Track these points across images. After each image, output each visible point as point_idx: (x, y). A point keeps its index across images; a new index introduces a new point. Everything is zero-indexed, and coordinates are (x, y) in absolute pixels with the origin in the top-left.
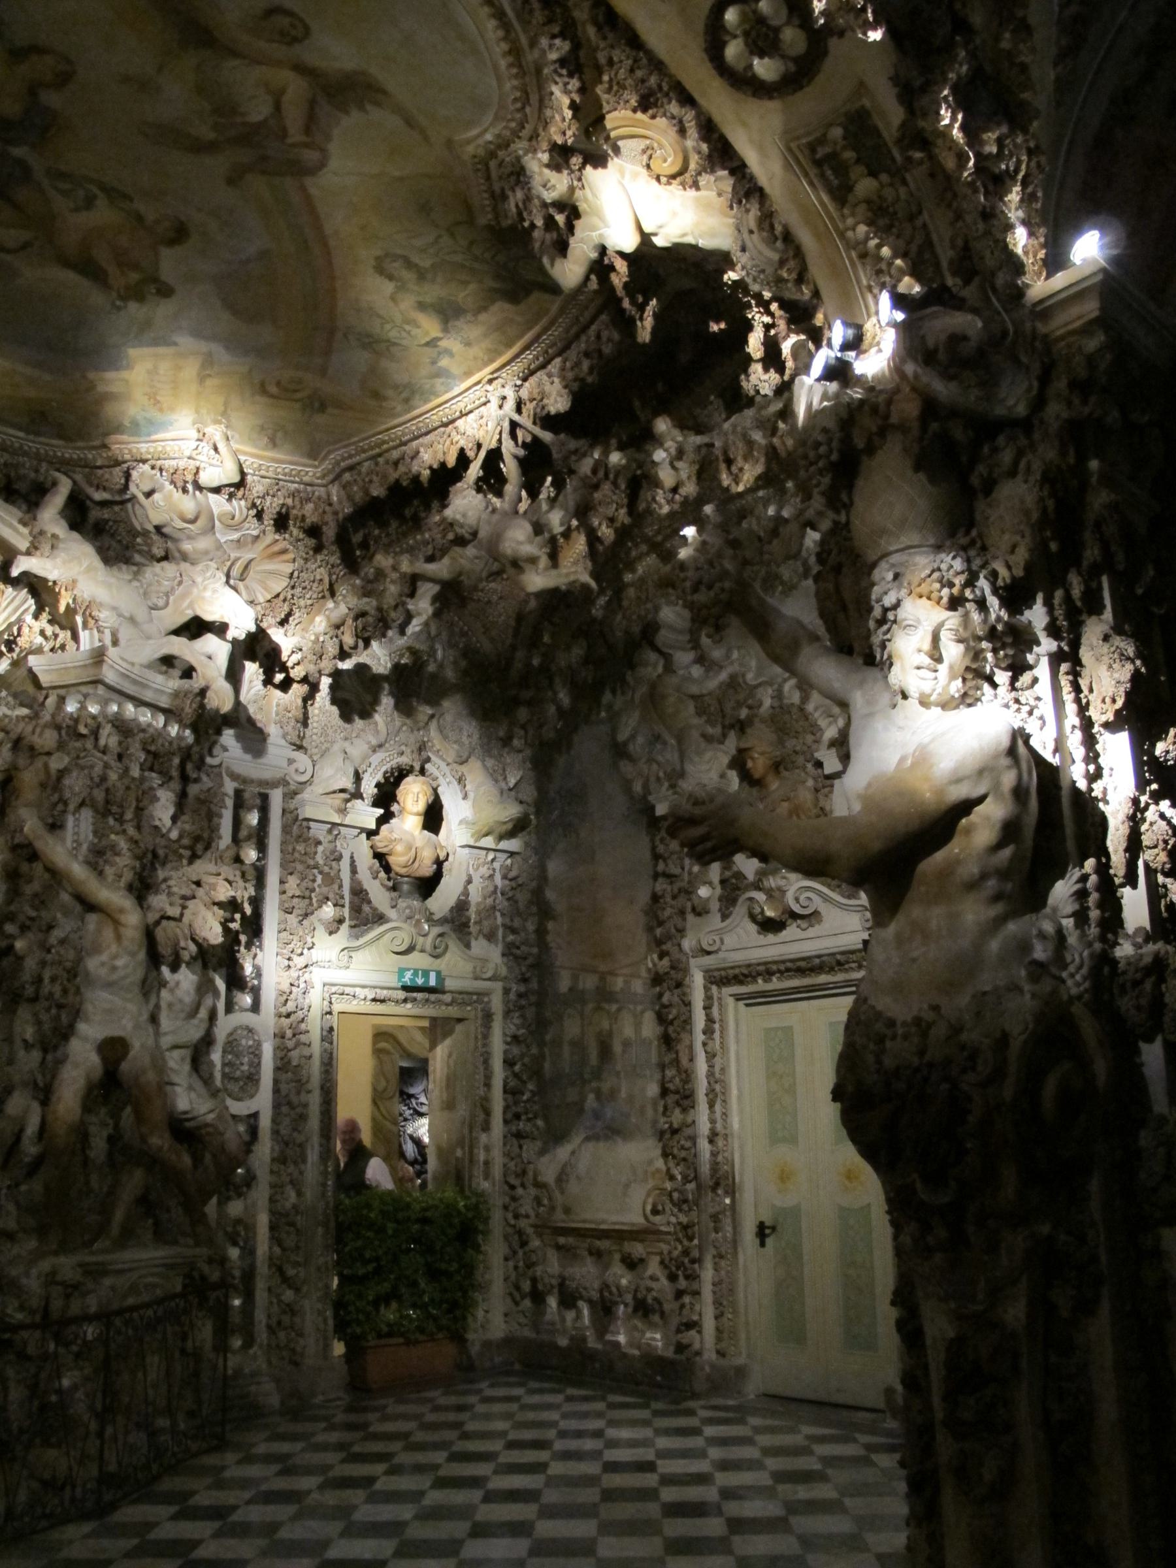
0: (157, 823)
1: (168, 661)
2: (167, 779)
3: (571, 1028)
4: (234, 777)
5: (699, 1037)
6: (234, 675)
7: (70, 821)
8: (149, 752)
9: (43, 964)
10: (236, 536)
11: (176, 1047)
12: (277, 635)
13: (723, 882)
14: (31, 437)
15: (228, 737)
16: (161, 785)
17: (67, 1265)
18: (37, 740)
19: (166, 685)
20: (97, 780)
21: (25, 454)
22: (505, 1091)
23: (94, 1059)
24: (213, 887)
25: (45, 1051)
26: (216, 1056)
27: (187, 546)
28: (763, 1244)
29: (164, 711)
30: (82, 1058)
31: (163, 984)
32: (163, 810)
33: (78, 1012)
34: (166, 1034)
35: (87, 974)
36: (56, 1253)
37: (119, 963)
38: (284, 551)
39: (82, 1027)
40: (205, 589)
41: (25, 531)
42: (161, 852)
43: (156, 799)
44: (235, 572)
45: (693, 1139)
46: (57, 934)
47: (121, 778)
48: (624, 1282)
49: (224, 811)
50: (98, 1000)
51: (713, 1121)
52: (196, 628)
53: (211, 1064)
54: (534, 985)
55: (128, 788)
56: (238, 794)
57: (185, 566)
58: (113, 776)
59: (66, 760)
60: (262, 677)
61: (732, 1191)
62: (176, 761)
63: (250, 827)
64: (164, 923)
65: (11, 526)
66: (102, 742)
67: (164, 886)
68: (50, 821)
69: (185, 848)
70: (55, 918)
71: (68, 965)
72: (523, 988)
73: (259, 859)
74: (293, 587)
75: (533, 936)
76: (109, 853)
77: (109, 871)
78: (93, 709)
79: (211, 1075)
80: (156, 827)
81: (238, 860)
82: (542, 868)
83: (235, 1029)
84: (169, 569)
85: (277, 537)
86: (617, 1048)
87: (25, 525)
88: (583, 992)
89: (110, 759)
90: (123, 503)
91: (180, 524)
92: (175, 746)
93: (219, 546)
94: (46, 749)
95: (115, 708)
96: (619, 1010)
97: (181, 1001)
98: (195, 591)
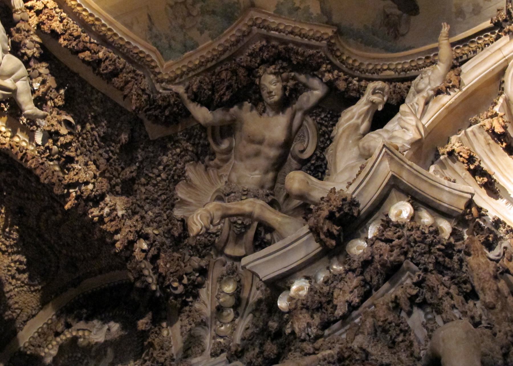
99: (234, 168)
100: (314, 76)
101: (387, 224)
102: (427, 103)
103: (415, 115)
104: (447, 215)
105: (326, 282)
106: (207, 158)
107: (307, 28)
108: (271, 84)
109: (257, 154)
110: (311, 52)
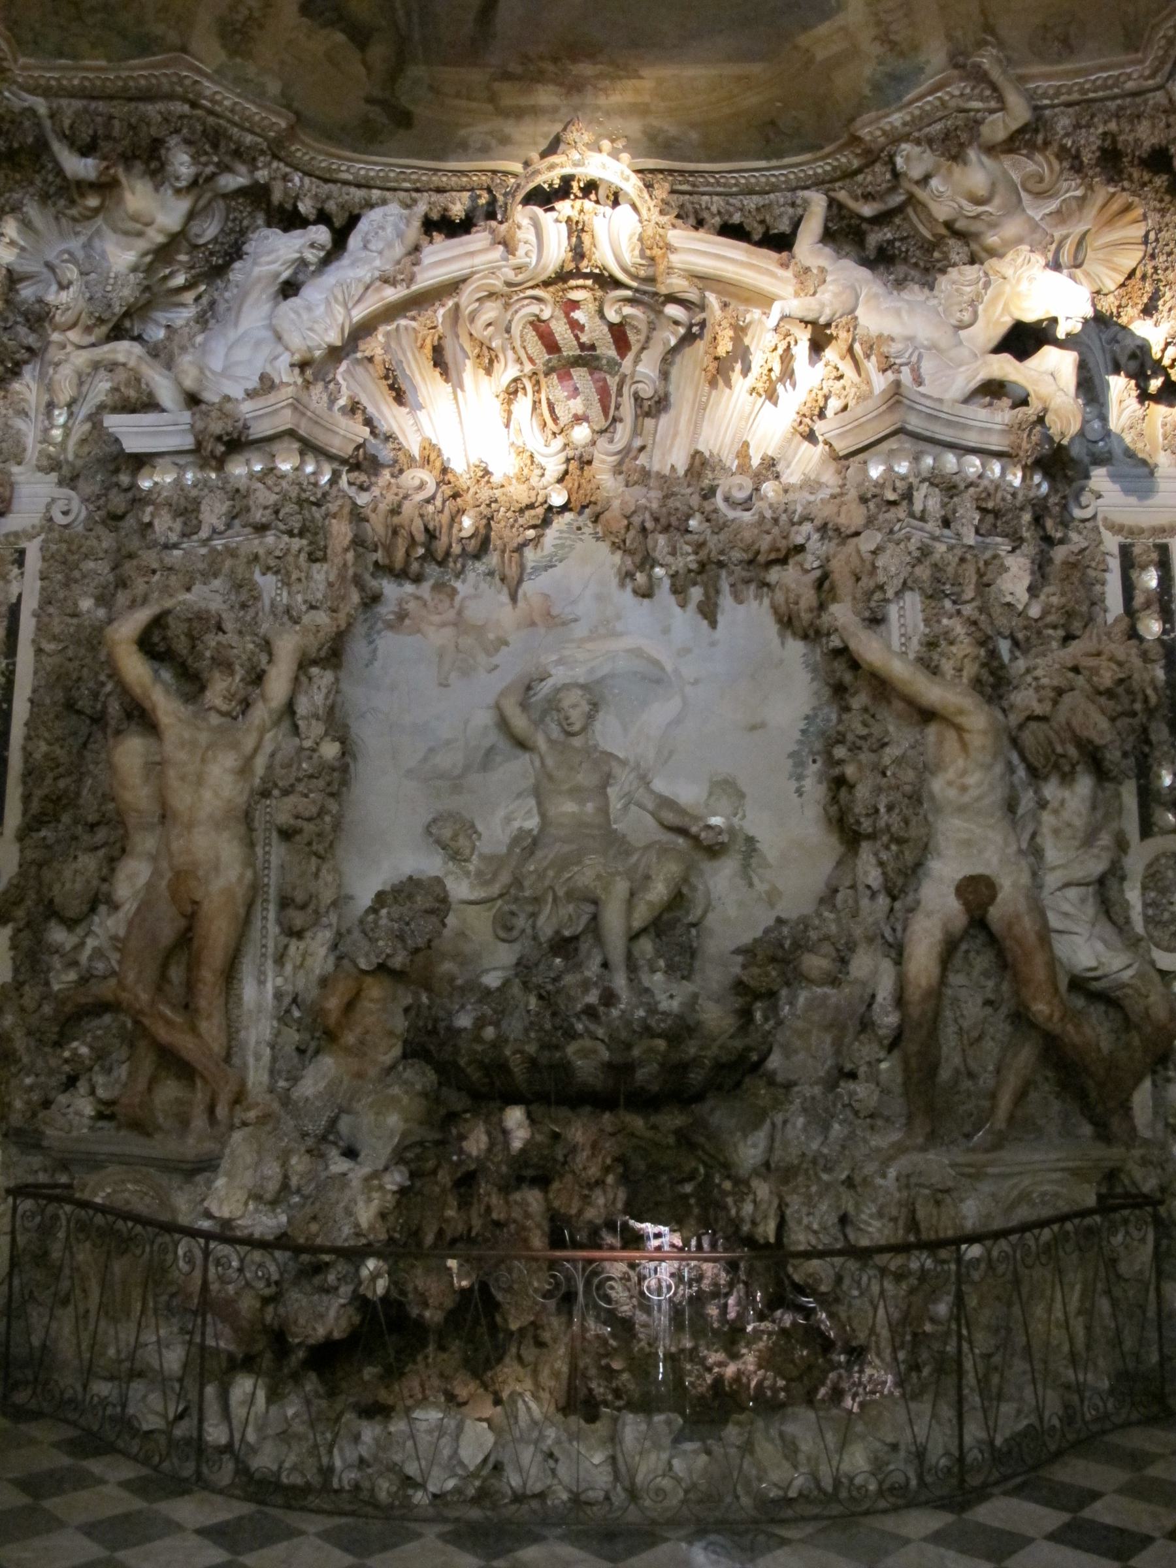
0: (1009, 599)
1: (993, 389)
2: (1017, 542)
4: (1117, 529)
6: (1089, 387)
7: (893, 611)
8: (983, 510)
9: (878, 790)
10: (1054, 205)
11: (1067, 885)
12: (1143, 329)
14: (774, 163)
15: (1099, 478)
16: (1013, 551)
17: (936, 1163)
18: (842, 520)
19: (992, 422)
20: (917, 554)
21: (774, 189)
23: (954, 905)
24: (1095, 671)
25: (894, 898)
26: (1133, 895)
27: (992, 239)
29: (999, 455)
30: (938, 903)
31: (1042, 804)
32: (1015, 579)
33: (926, 847)
34: (1053, 869)
35: (932, 798)
36: (923, 1149)
37: (971, 780)
38: (1127, 208)
39: (935, 866)
40: (1019, 280)
41: (788, 274)
42: (1020, 636)
43: (1005, 569)
44: (1065, 258)
46: (891, 752)
47: (951, 548)
49: (1108, 576)
50: (951, 830)
52: (1024, 339)
53: (1126, 905)
55: (962, 560)
56: (1125, 552)
57: (993, 262)
58: (941, 548)
59: (879, 537)
60: (1135, 393)
62: (1027, 517)
63: (1147, 591)
64: (1033, 725)
65: (772, 275)
66: (918, 507)
67: (1029, 679)
68: (867, 614)
69: (1055, 627)
70: (887, 732)
71: (908, 788)
73: (1165, 632)
74: (1153, 256)
76: (943, 643)
77: (947, 667)
78: (903, 468)
79: (1128, 921)
80: (1009, 604)
81: (1133, 634)
83: (1157, 859)
84: (972, 272)
85: (1112, 190)
87: (785, 265)
89: (932, 526)
90: (900, 209)
91: (972, 210)
92: (1020, 497)
93: (1034, 226)
94: (853, 529)
95: (929, 461)
97: (1069, 825)
98: (1008, 288)
99: (98, 232)
100: (244, 162)
101: (271, 470)
102: (367, 288)
103: (345, 305)
104: (331, 457)
105: (195, 486)
106: (62, 202)
107: (254, 109)
108: (182, 164)
109: (140, 234)
110: (249, 139)
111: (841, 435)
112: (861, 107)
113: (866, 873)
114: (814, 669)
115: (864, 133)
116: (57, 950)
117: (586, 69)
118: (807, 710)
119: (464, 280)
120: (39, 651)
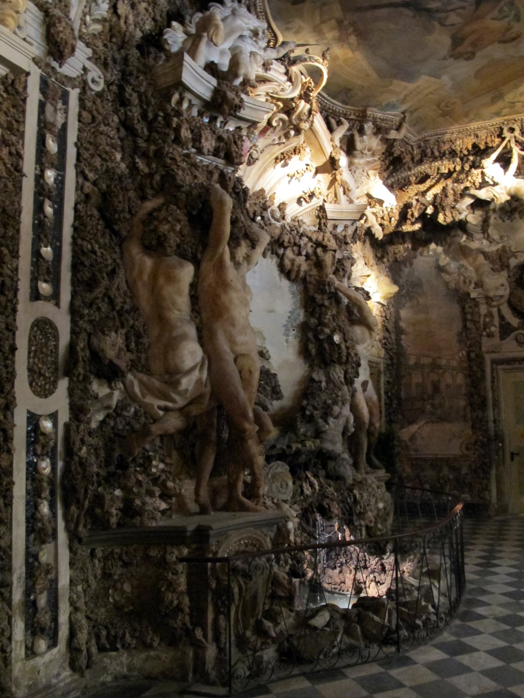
3: (417, 379)
5: (489, 384)
13: (501, 326)
14: (329, 98)
22: (385, 404)
28: (512, 460)
45: (487, 422)
48: (451, 477)
51: (494, 415)
54: (395, 361)
61: (503, 441)
72: (389, 362)
75: (394, 341)
82: (397, 313)
86: (443, 386)
88: (423, 365)
96: (444, 372)
111: (333, 212)
112: (376, 106)
113: (339, 377)
114: (293, 294)
115: (369, 113)
116: (96, 397)
117: (353, 39)
118: (290, 309)
119: (269, 81)
120: (81, 173)
